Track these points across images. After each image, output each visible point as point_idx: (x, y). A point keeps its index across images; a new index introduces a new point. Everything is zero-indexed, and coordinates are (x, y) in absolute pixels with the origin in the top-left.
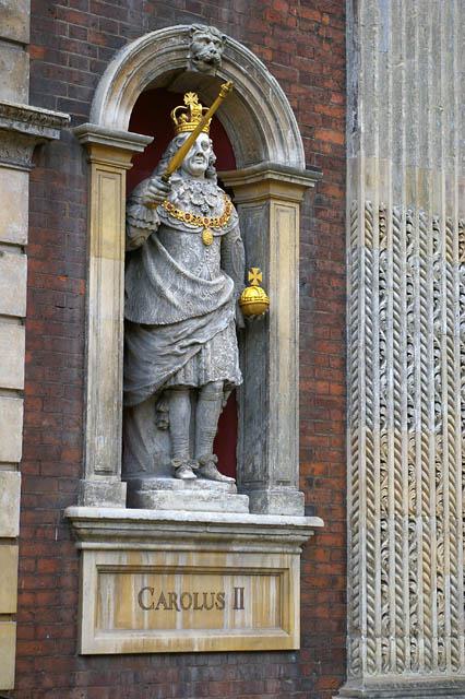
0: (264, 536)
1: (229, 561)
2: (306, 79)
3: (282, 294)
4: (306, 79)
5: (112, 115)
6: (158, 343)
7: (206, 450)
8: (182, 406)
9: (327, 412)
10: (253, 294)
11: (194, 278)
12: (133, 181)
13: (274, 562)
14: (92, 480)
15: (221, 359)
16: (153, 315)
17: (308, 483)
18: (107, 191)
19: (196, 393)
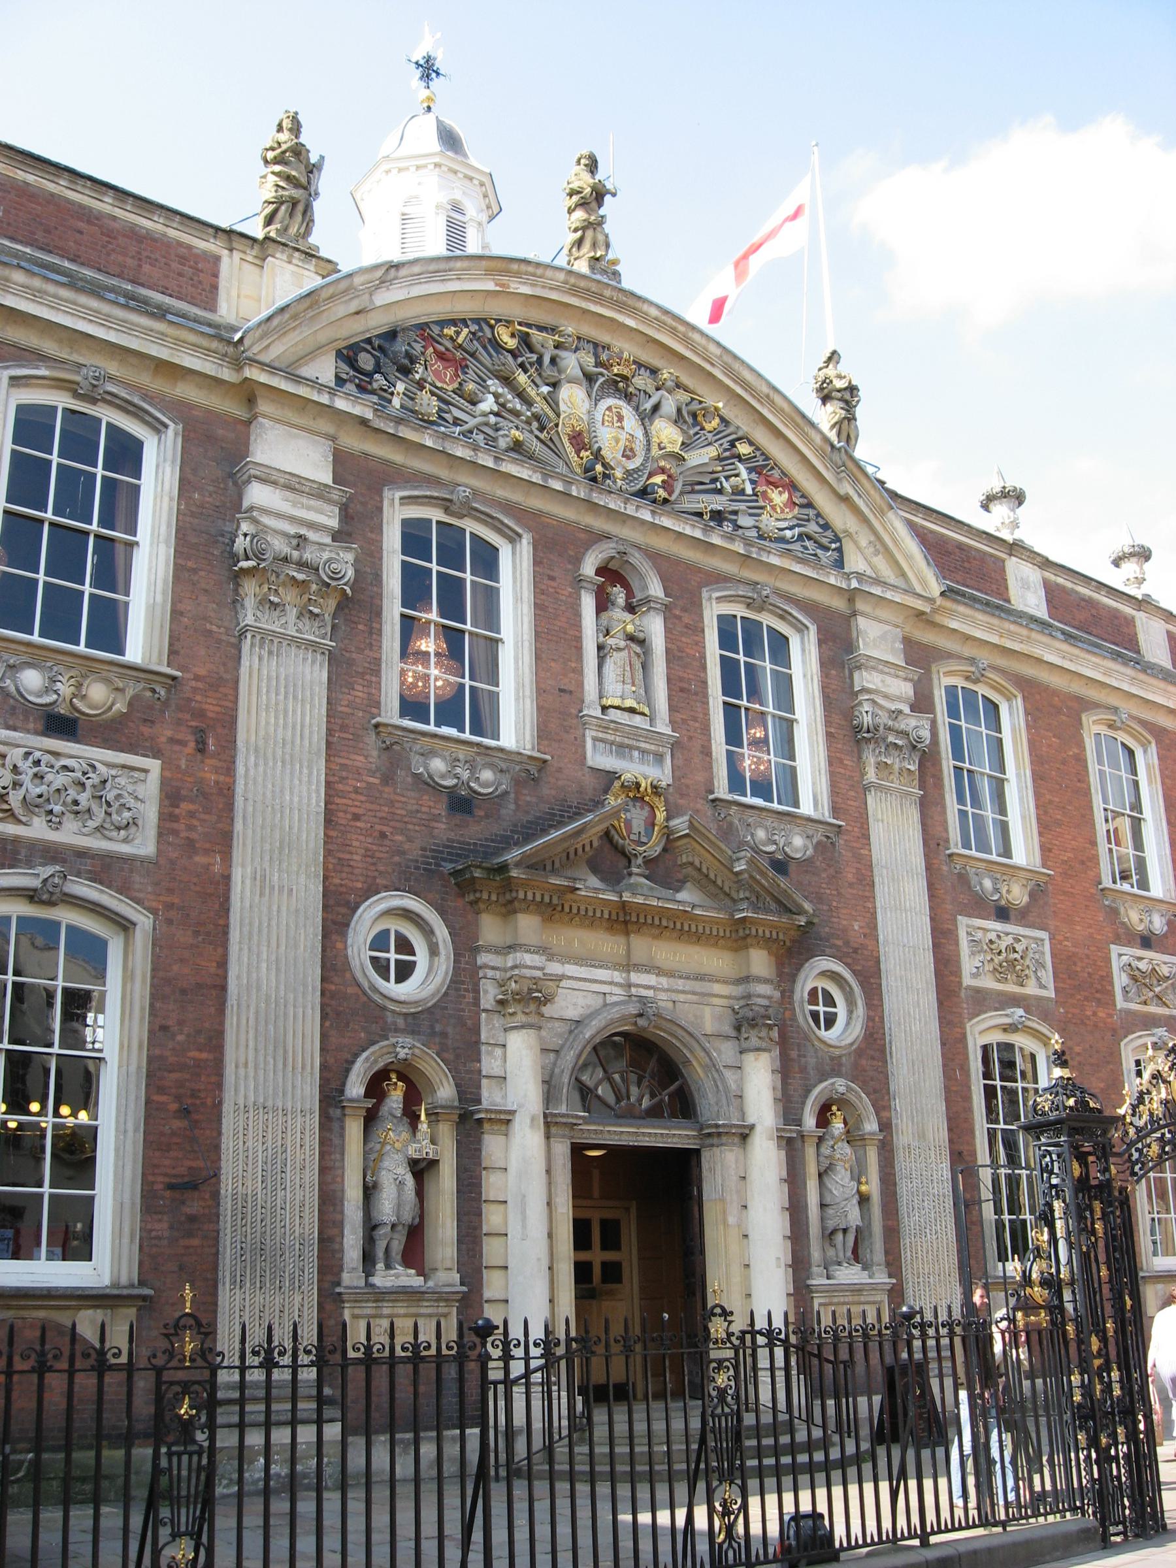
0: (874, 1287)
1: (862, 1299)
2: (875, 1091)
3: (872, 1186)
4: (875, 1091)
6: (830, 1211)
7: (849, 1253)
8: (839, 1237)
9: (892, 1233)
10: (863, 1188)
11: (842, 1184)
12: (818, 1145)
13: (878, 1298)
14: (815, 1269)
15: (854, 1217)
16: (828, 1200)
17: (888, 1264)
18: (810, 1151)
19: (845, 1231)
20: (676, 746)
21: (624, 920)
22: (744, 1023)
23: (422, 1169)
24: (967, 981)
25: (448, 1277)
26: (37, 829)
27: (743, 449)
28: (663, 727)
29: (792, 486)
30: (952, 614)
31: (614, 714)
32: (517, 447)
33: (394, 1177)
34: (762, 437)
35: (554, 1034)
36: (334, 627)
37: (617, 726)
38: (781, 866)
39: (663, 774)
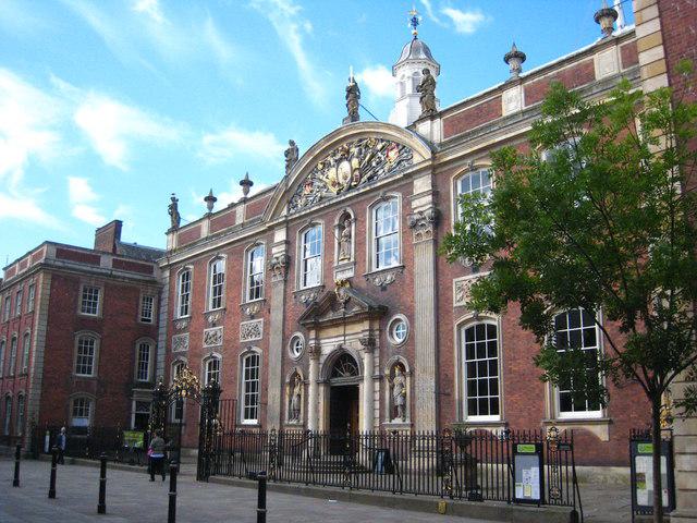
5: (387, 372)
9: (413, 407)
20: (355, 263)
21: (334, 324)
22: (370, 344)
23: (299, 396)
24: (455, 305)
25: (302, 421)
26: (250, 339)
27: (379, 146)
28: (352, 260)
29: (398, 145)
30: (446, 156)
31: (341, 263)
32: (321, 198)
33: (295, 398)
34: (387, 138)
35: (322, 360)
36: (286, 274)
37: (340, 267)
38: (384, 288)
39: (350, 274)
